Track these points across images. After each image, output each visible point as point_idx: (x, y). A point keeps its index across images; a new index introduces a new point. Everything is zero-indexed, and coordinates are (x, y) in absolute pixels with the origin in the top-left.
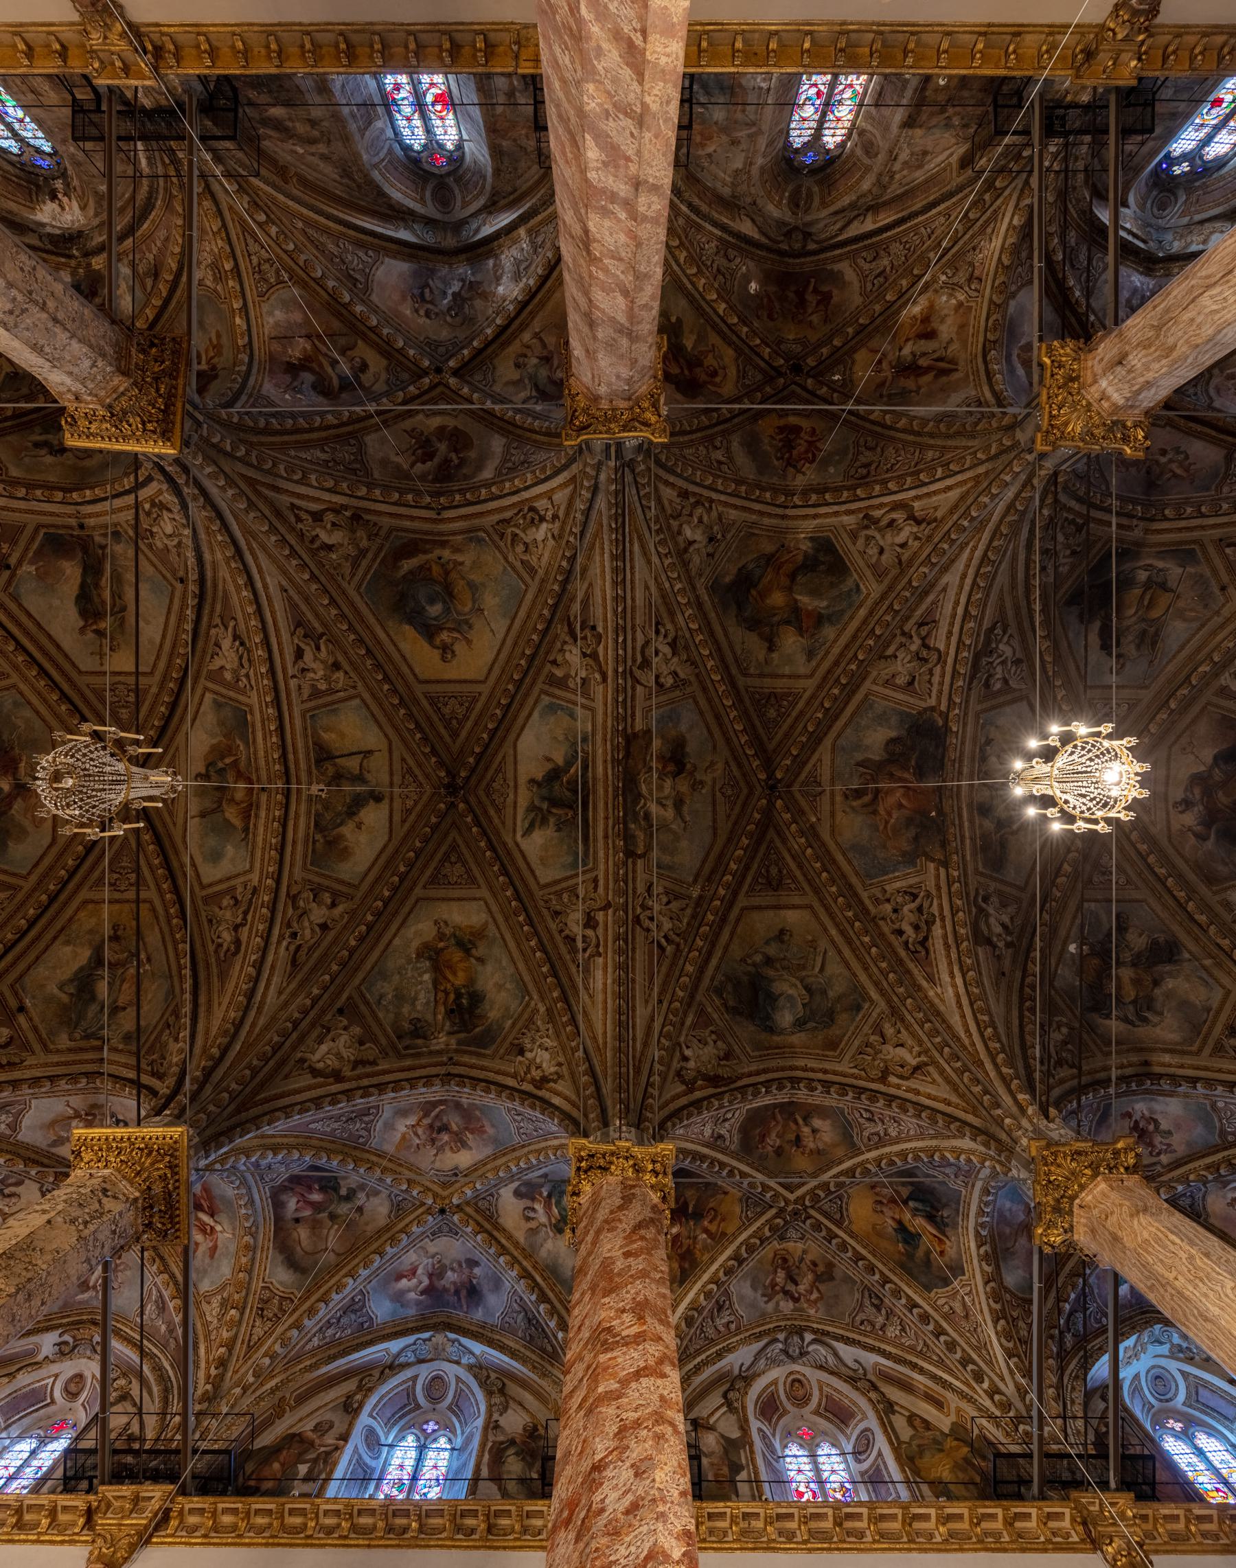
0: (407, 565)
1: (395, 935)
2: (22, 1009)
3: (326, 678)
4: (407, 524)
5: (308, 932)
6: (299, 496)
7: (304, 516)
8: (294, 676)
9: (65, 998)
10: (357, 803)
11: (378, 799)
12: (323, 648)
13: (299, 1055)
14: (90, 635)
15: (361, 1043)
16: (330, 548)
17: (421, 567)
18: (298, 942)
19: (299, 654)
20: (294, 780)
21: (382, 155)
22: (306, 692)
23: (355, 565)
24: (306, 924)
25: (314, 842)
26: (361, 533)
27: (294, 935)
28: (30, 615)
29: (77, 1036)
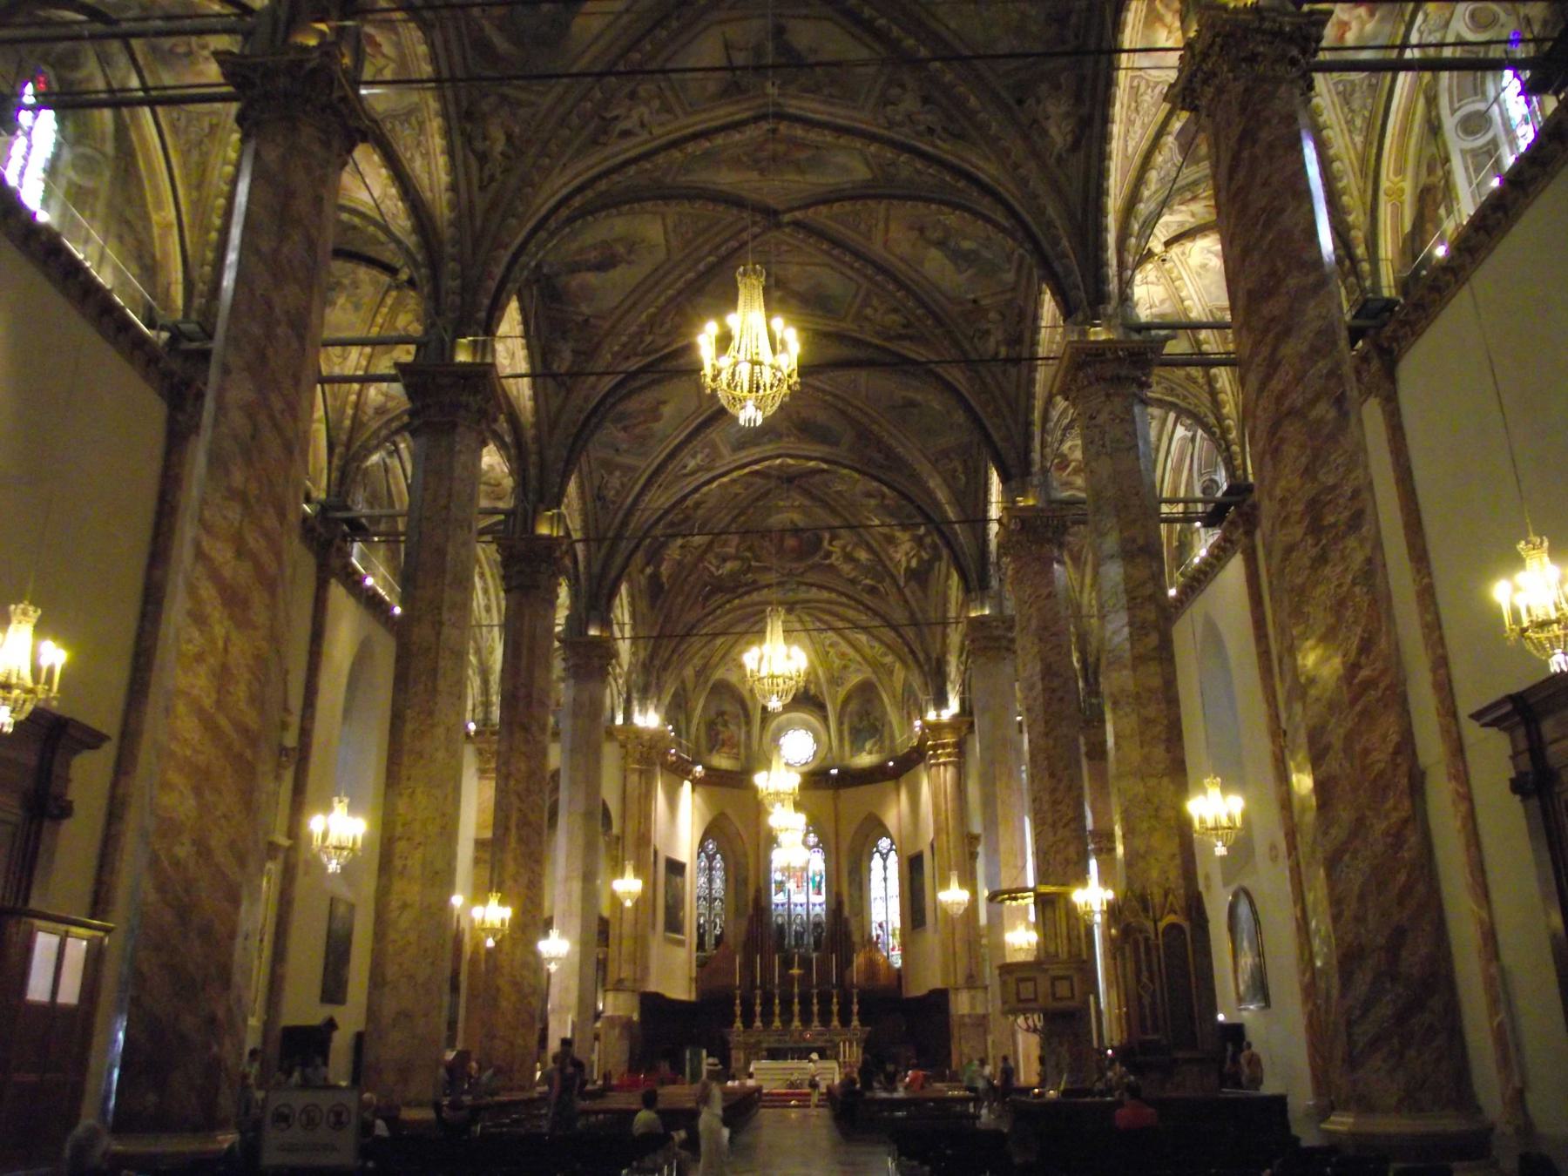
0: (501, 43)
1: (948, 28)
2: (975, 301)
3: (647, 103)
4: (457, 58)
5: (929, 118)
6: (469, 183)
7: (486, 173)
8: (651, 133)
9: (970, 272)
10: (785, 49)
11: (780, 31)
12: (615, 113)
13: (1053, 160)
14: (633, 257)
15: (1057, 87)
16: (509, 137)
17: (500, 28)
18: (939, 129)
19: (626, 134)
20: (764, 110)
21: (89, 151)
22: (665, 117)
23: (519, 104)
24: (921, 117)
25: (831, 96)
26: (485, 106)
27: (931, 131)
28: (623, 301)
29: (1007, 267)
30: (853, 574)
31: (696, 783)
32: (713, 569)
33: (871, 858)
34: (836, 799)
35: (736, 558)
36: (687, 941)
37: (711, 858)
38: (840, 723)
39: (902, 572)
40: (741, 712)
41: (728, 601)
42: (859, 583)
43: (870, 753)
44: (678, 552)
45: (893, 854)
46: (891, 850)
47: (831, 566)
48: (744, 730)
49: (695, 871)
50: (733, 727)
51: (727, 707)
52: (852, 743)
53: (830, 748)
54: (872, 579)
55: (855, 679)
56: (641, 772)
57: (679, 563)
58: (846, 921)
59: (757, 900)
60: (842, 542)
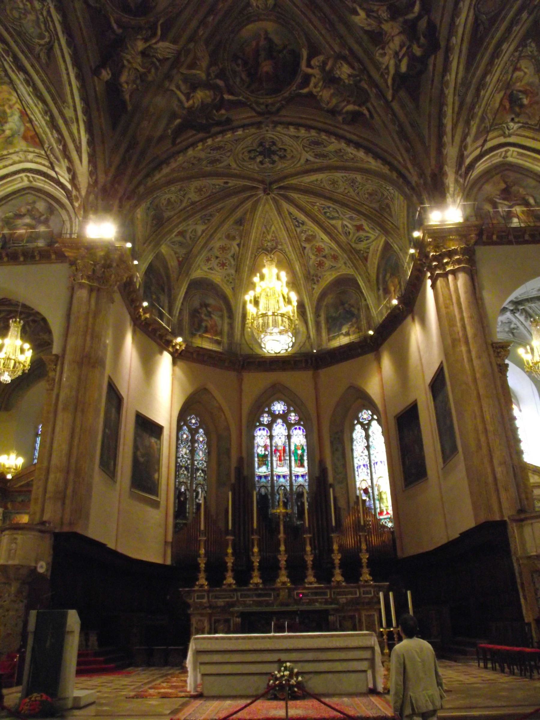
30: (334, 101)
31: (177, 357)
32: (183, 98)
34: (315, 378)
35: (208, 85)
36: (163, 503)
37: (193, 432)
38: (317, 315)
39: (390, 81)
40: (224, 307)
41: (203, 140)
42: (340, 113)
43: (347, 334)
44: (139, 59)
47: (311, 95)
48: (226, 320)
50: (215, 317)
51: (211, 301)
52: (329, 330)
53: (309, 337)
54: (354, 103)
55: (329, 277)
56: (91, 290)
57: (142, 77)
60: (321, 58)
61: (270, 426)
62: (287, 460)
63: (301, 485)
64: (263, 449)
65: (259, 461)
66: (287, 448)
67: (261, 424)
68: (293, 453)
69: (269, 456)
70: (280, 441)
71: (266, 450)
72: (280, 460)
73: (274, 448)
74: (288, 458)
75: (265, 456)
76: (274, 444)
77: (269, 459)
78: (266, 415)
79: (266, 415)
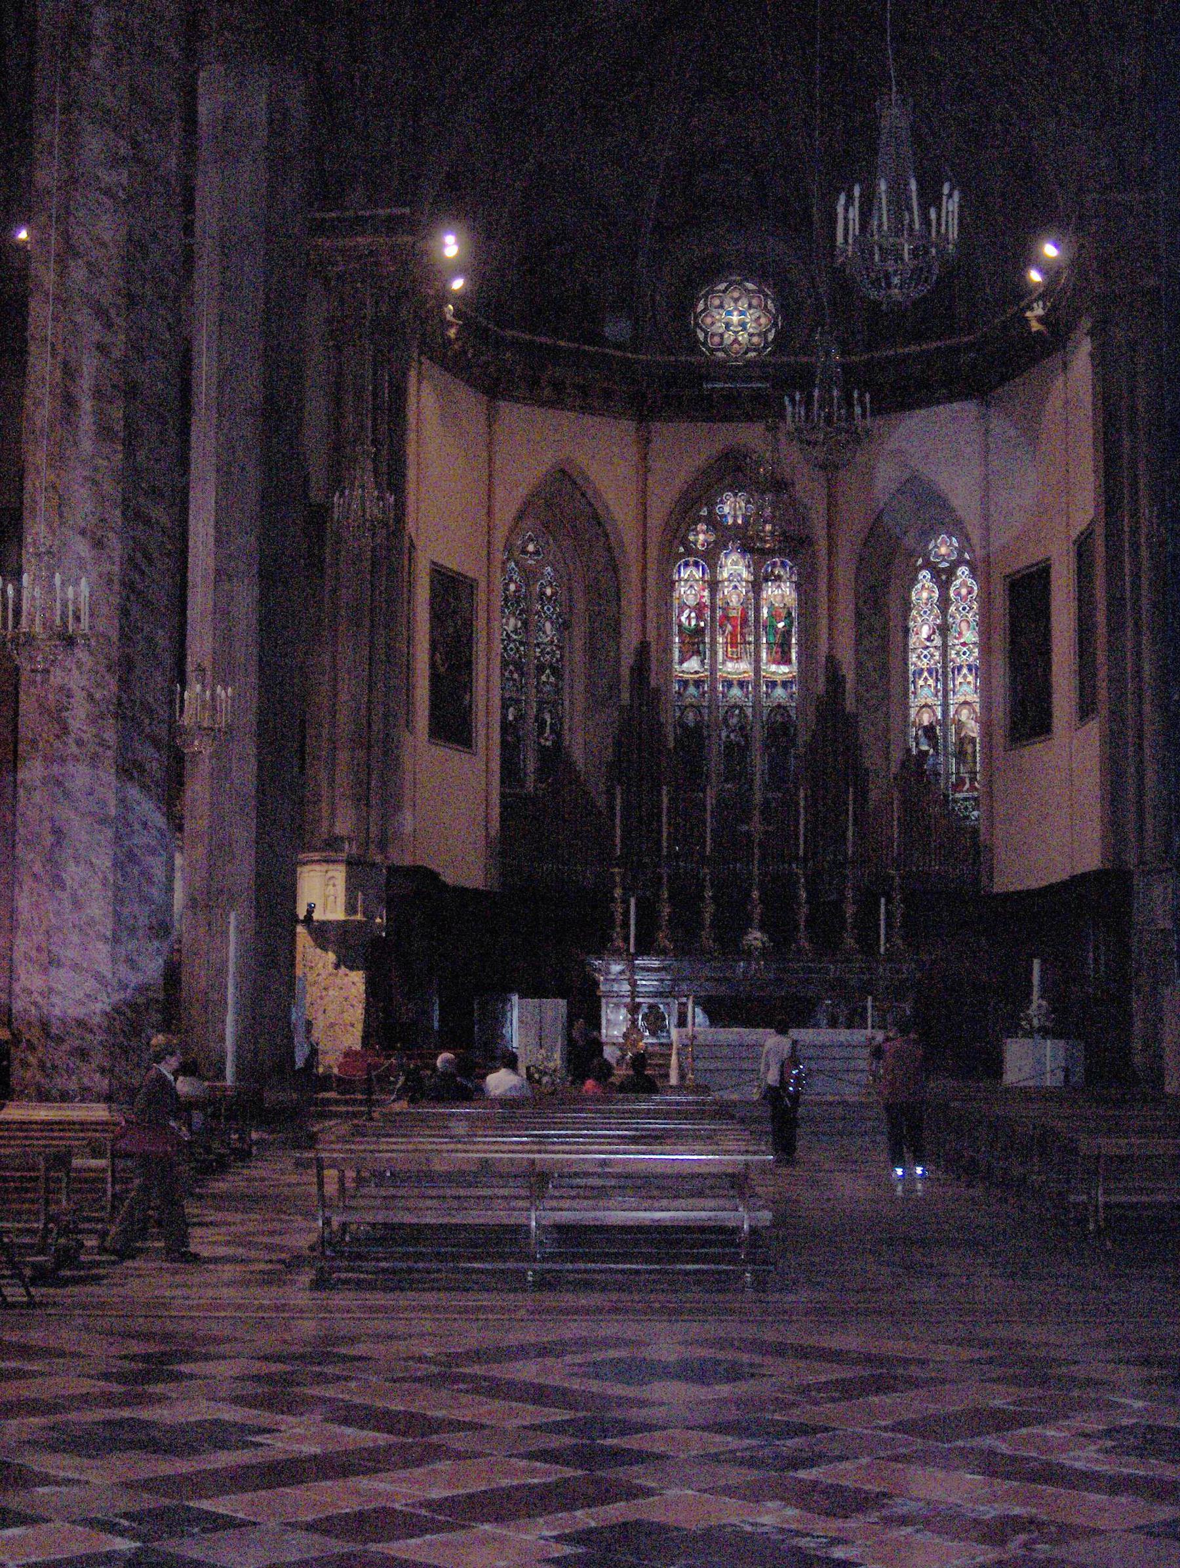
33: (914, 580)
45: (963, 571)
46: (960, 562)
49: (498, 602)
58: (850, 722)
59: (641, 669)
61: (710, 557)
62: (750, 643)
63: (779, 706)
64: (693, 615)
65: (682, 642)
66: (751, 613)
67: (690, 552)
68: (765, 627)
69: (707, 632)
70: (734, 595)
71: (698, 618)
72: (734, 645)
73: (719, 613)
74: (751, 639)
75: (699, 631)
76: (719, 603)
77: (707, 640)
78: (702, 527)
79: (702, 527)
